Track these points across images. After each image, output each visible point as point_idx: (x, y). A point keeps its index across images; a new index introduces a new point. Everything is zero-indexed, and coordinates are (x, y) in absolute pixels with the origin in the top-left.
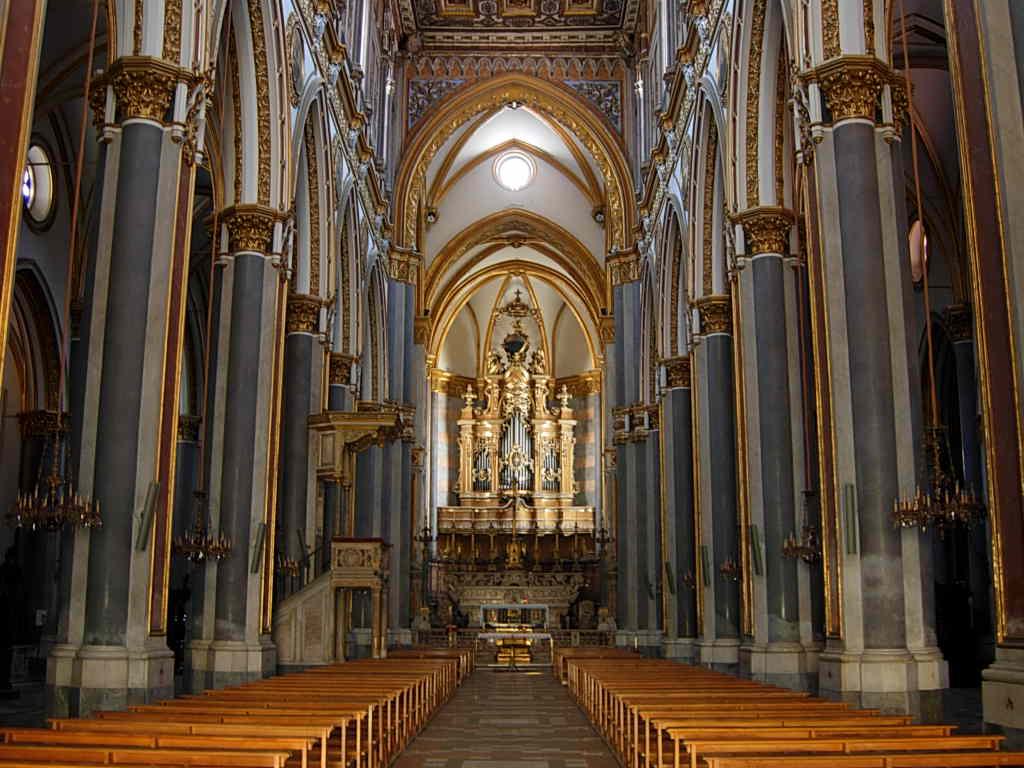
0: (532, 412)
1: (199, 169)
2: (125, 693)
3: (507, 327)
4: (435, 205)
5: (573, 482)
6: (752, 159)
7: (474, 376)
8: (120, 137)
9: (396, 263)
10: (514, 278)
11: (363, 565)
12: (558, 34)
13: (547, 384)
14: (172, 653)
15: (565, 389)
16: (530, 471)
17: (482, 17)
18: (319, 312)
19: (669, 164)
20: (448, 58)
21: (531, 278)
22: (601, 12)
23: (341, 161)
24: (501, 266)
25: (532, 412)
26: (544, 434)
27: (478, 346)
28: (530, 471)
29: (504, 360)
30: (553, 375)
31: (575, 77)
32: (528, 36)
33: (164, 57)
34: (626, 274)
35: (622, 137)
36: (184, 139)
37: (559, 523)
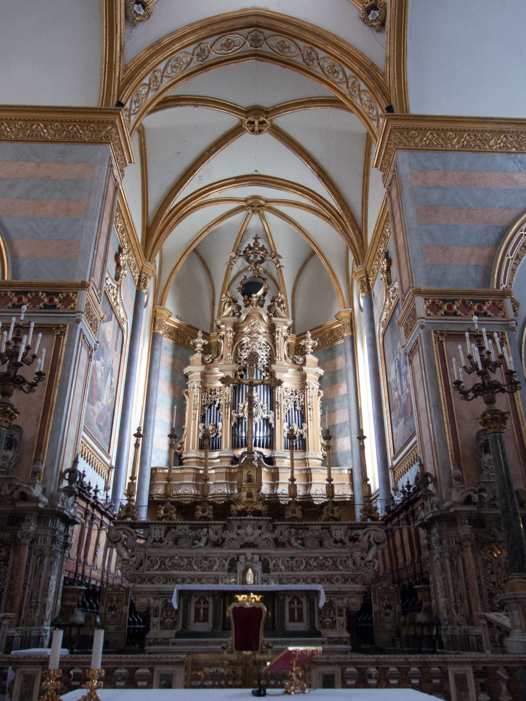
0: (272, 359)
15: (309, 335)
16: (269, 425)
25: (272, 359)
27: (213, 304)
28: (269, 425)
29: (241, 303)
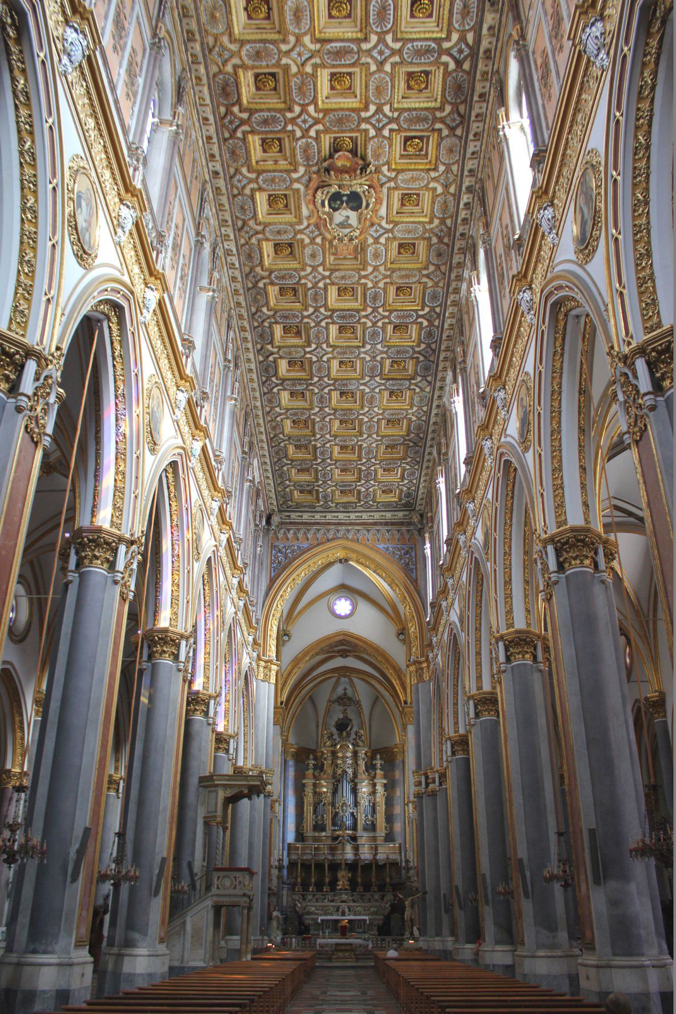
0: (355, 774)
1: (131, 603)
2: (54, 994)
3: (338, 714)
4: (289, 628)
5: (384, 825)
6: (509, 597)
7: (314, 747)
8: (78, 580)
9: (261, 669)
10: (343, 679)
11: (235, 888)
12: (372, 514)
13: (366, 754)
14: (92, 959)
17: (322, 503)
18: (209, 703)
19: (450, 601)
20: (298, 530)
21: (355, 680)
22: (400, 499)
23: (226, 598)
24: (334, 670)
25: (355, 774)
26: (364, 790)
27: (318, 726)
30: (370, 747)
31: (384, 542)
32: (353, 516)
33: (111, 527)
34: (421, 676)
35: (416, 581)
36: (121, 582)
37: (376, 854)
